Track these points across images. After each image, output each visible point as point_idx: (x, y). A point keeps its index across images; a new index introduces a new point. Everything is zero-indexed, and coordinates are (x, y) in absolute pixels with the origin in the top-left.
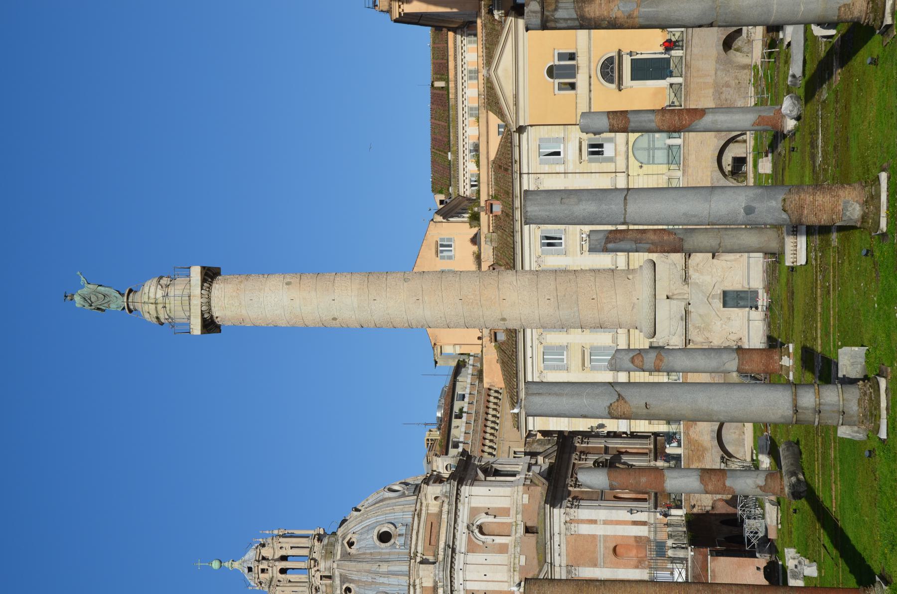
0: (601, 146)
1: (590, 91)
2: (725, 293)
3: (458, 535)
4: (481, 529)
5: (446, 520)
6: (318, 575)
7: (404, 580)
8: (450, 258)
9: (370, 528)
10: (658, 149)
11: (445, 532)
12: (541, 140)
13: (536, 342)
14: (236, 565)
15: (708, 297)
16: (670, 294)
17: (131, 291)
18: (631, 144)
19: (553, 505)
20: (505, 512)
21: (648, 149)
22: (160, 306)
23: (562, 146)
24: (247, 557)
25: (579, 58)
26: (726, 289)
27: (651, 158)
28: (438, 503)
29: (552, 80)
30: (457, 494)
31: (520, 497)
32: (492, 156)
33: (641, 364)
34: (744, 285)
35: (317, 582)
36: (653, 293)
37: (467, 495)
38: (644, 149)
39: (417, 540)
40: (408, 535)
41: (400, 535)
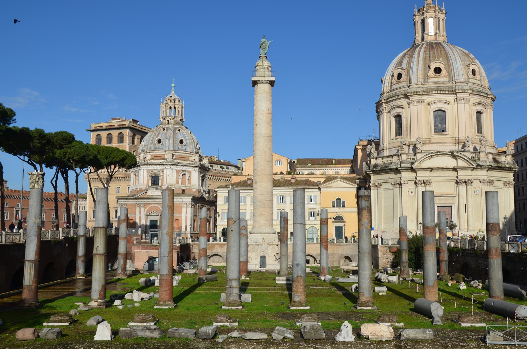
0: (314, 216)
1: (332, 212)
3: (182, 167)
4: (184, 174)
6: (169, 119)
7: (167, 148)
8: (275, 165)
10: (312, 235)
14: (173, 92)
16: (264, 239)
17: (267, 57)
19: (192, 199)
20: (190, 183)
21: (312, 232)
22: (261, 67)
24: (175, 95)
28: (193, 160)
30: (196, 167)
31: (195, 188)
32: (310, 179)
35: (167, 119)
38: (312, 230)
39: (181, 153)
40: (182, 150)
41: (182, 147)
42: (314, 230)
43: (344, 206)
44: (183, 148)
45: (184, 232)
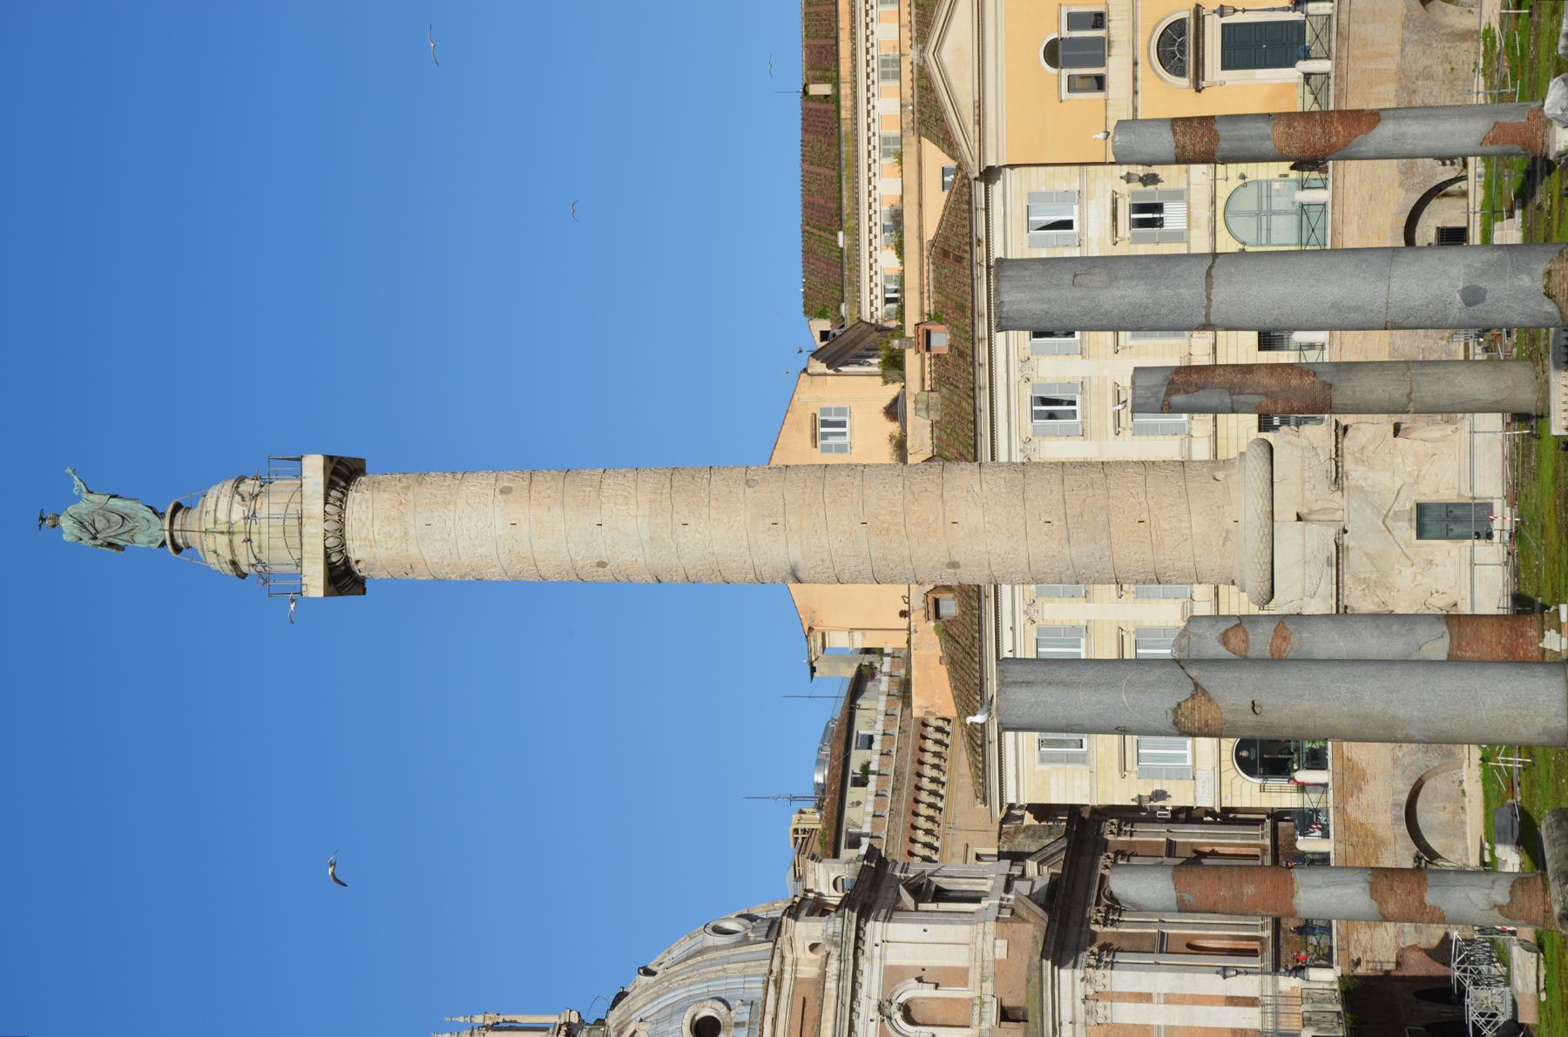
0: (1158, 208)
1: (1135, 92)
2: (1421, 509)
5: (834, 993)
8: (842, 449)
9: (677, 1010)
10: (1279, 213)
11: (831, 1018)
12: (1031, 196)
13: (1021, 619)
15: (1386, 516)
16: (1304, 511)
17: (178, 507)
18: (1220, 204)
19: (1059, 963)
20: (958, 976)
22: (238, 539)
23: (1076, 208)
25: (1111, 25)
26: (1424, 499)
27: (1264, 232)
28: (818, 957)
29: (1054, 71)
30: (858, 938)
31: (989, 946)
32: (930, 233)
33: (1243, 646)
34: (1463, 492)
36: (1269, 509)
37: (878, 941)
38: (1249, 214)
41: (738, 1025)
42: (1248, 201)
43: (1099, 20)
44: (746, 1018)
45: (1269, 1017)
